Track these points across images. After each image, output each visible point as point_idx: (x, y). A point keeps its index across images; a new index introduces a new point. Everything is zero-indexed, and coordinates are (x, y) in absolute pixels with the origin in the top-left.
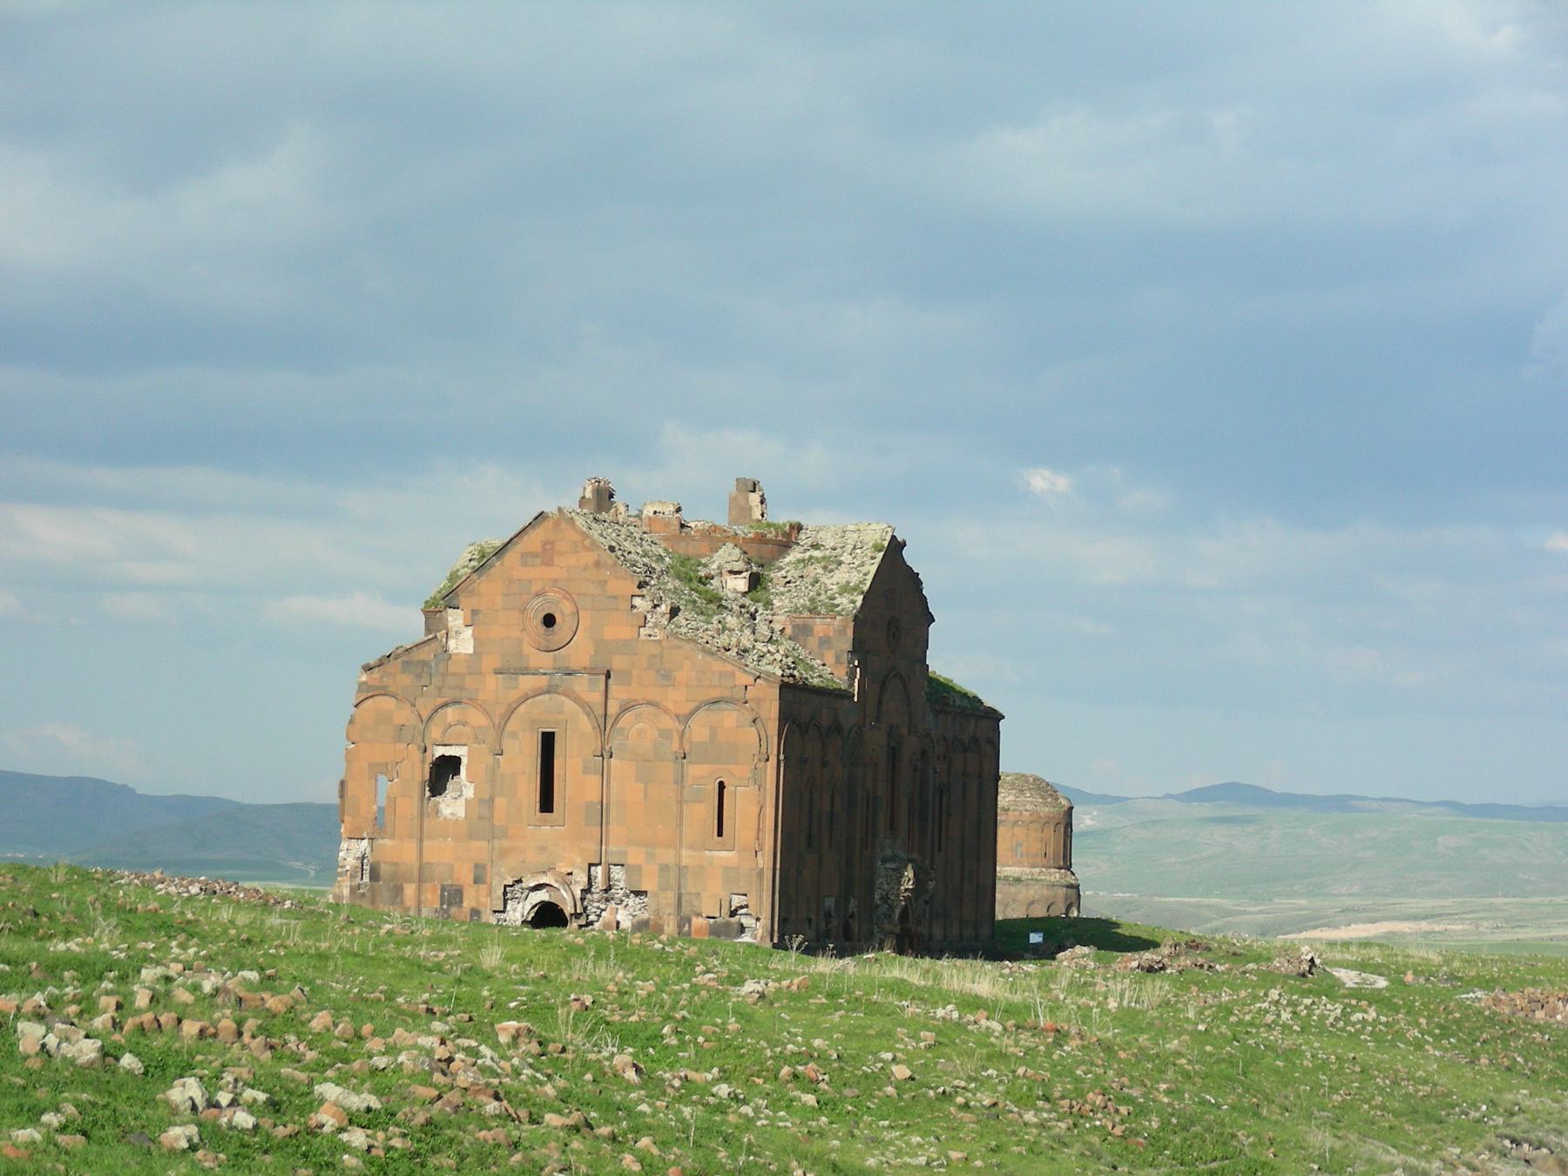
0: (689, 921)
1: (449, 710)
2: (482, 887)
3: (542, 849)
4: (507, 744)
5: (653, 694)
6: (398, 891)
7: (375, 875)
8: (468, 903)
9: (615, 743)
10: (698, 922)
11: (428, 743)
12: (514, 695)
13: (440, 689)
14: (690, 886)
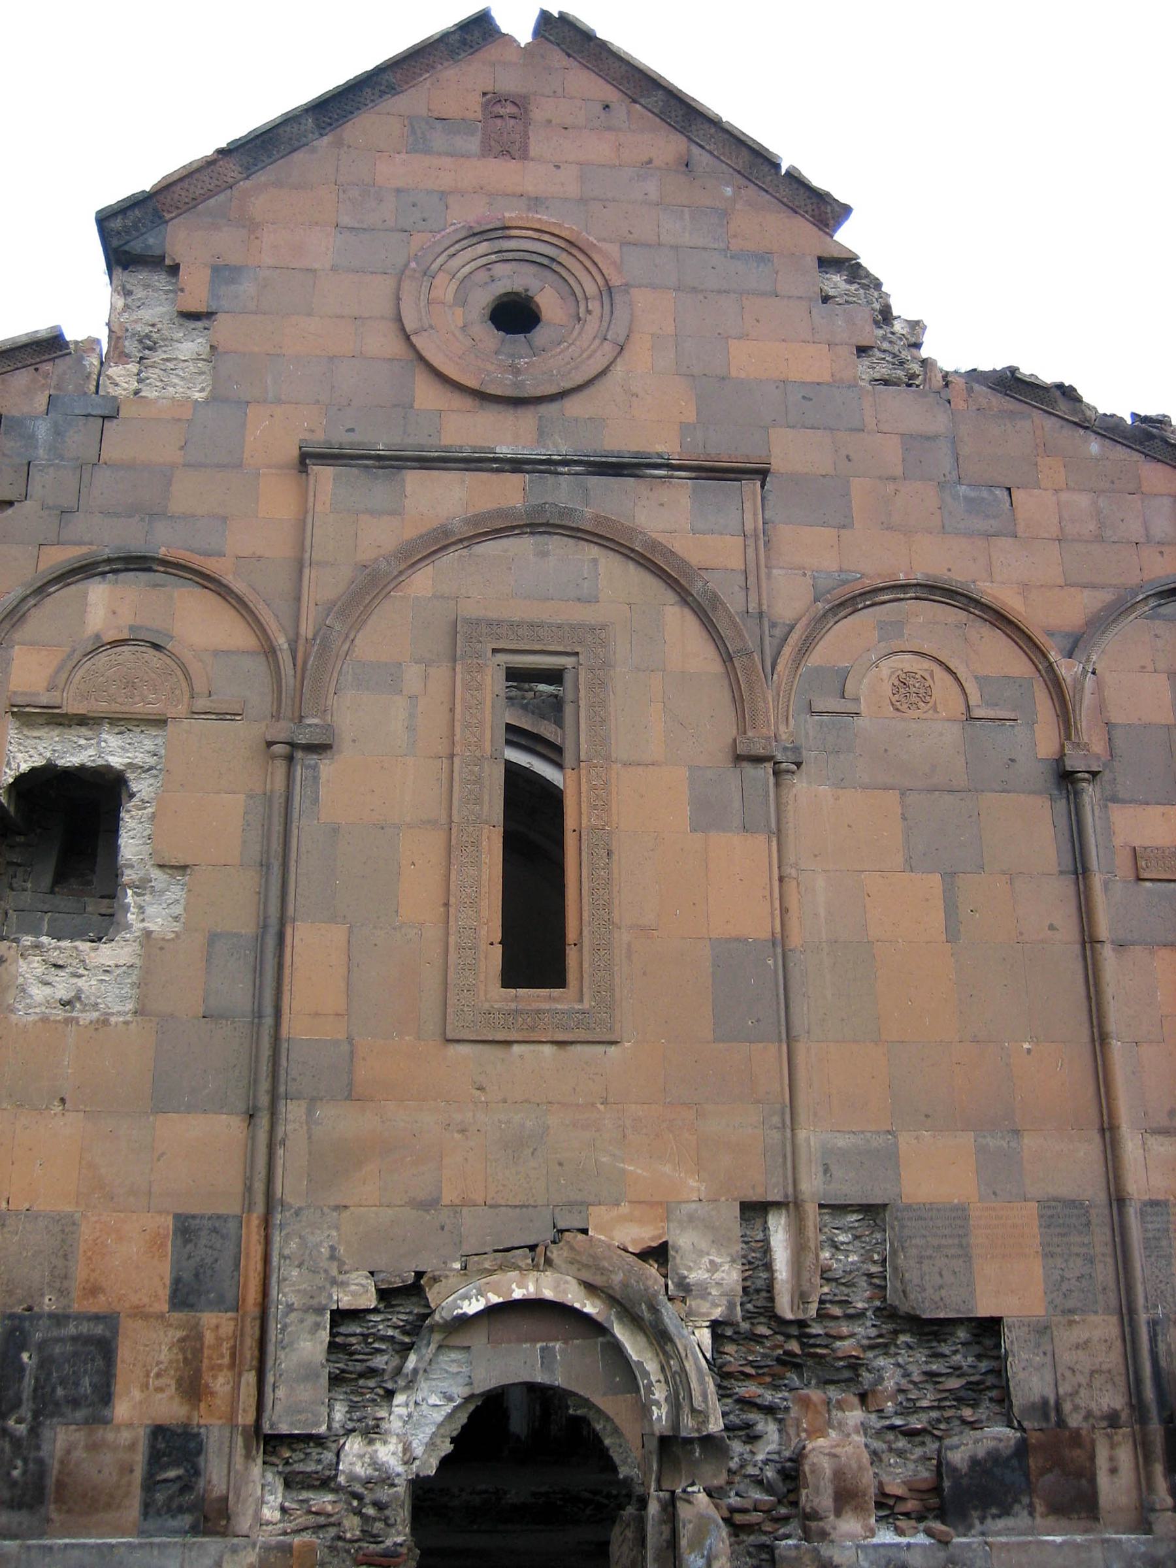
4: (352, 712)
12: (380, 537)
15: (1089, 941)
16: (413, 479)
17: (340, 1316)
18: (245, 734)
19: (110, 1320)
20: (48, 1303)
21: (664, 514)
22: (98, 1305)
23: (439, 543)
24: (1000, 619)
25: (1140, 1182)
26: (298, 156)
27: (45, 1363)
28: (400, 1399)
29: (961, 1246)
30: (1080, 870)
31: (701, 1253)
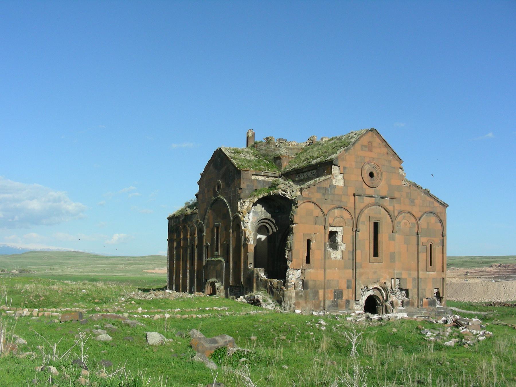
0: (422, 300)
1: (336, 211)
2: (350, 290)
3: (375, 273)
4: (360, 227)
5: (409, 208)
6: (316, 293)
7: (305, 285)
8: (345, 298)
9: (396, 228)
10: (425, 300)
11: (327, 225)
12: (362, 206)
13: (332, 201)
14: (422, 286)
15: (418, 252)
16: (365, 198)
18: (350, 228)
19: (342, 290)
20: (337, 288)
21: (386, 203)
23: (368, 206)
24: (414, 216)
25: (420, 276)
30: (418, 245)
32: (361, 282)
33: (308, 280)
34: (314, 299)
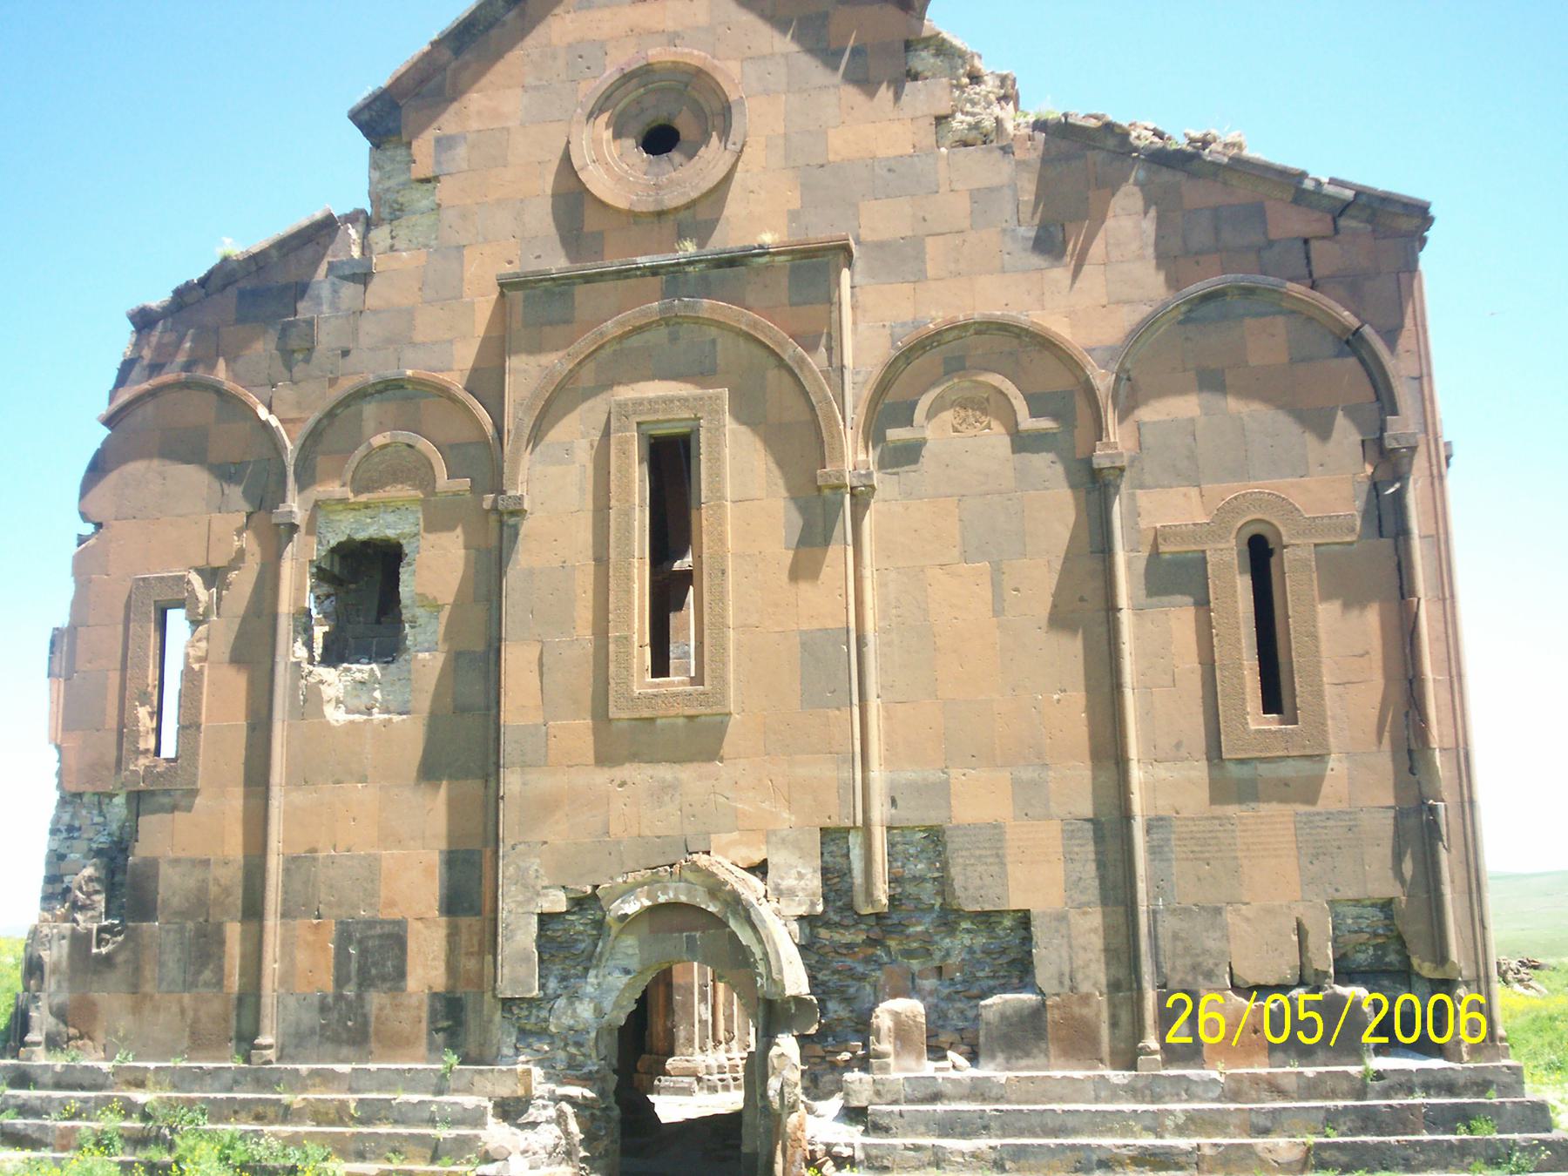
17: (545, 919)
19: (401, 924)
22: (395, 914)
26: (494, 32)
27: (364, 952)
28: (592, 973)
29: (998, 856)
31: (791, 867)
32: (534, 864)
33: (152, 865)
34: (194, 984)
